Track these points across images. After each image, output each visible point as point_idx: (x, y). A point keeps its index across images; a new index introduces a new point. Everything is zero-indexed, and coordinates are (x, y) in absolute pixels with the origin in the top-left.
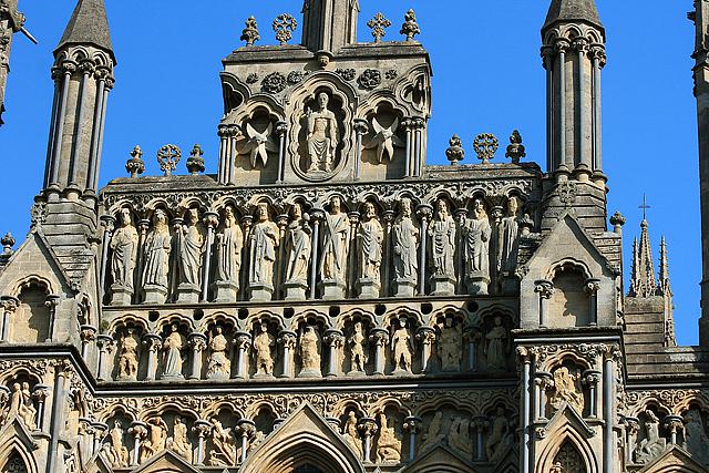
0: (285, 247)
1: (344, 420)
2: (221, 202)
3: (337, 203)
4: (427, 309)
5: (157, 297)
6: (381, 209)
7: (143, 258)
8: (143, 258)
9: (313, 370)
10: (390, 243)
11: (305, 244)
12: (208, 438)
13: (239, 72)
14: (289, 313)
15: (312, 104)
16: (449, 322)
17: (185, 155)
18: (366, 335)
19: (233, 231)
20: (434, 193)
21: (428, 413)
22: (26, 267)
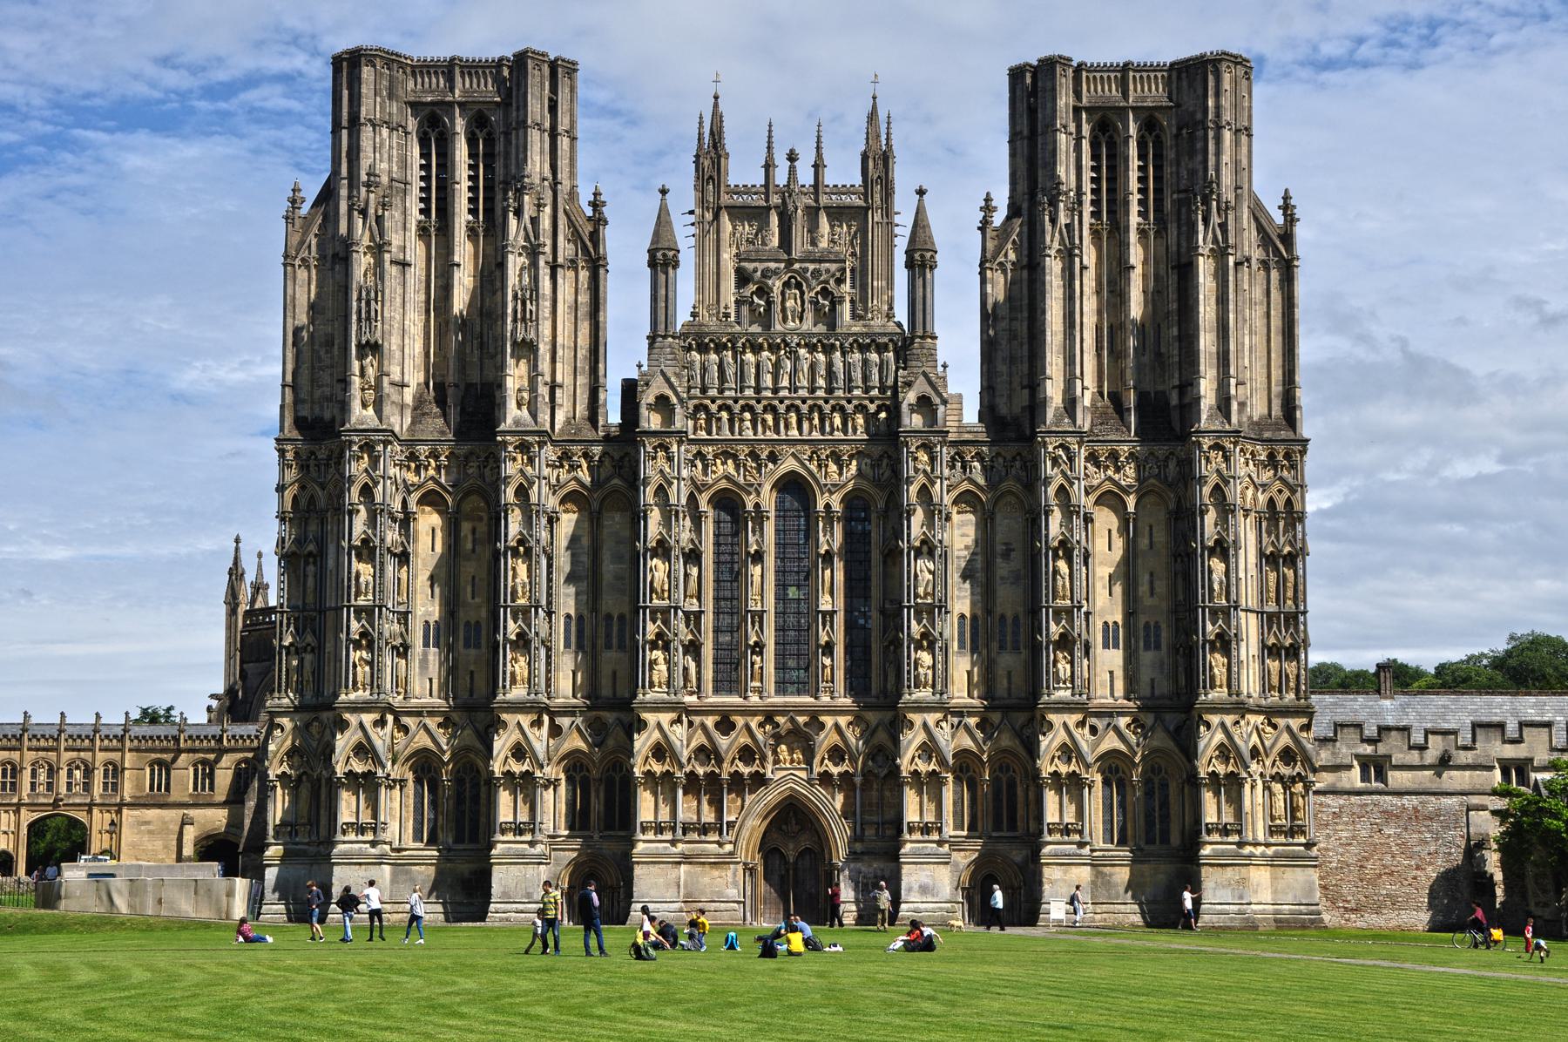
0: (777, 366)
1: (811, 459)
5: (713, 392)
6: (823, 346)
7: (704, 369)
8: (704, 369)
9: (794, 433)
10: (830, 365)
11: (788, 364)
12: (745, 465)
13: (749, 266)
15: (787, 285)
19: (749, 357)
20: (851, 340)
21: (851, 457)
22: (658, 387)
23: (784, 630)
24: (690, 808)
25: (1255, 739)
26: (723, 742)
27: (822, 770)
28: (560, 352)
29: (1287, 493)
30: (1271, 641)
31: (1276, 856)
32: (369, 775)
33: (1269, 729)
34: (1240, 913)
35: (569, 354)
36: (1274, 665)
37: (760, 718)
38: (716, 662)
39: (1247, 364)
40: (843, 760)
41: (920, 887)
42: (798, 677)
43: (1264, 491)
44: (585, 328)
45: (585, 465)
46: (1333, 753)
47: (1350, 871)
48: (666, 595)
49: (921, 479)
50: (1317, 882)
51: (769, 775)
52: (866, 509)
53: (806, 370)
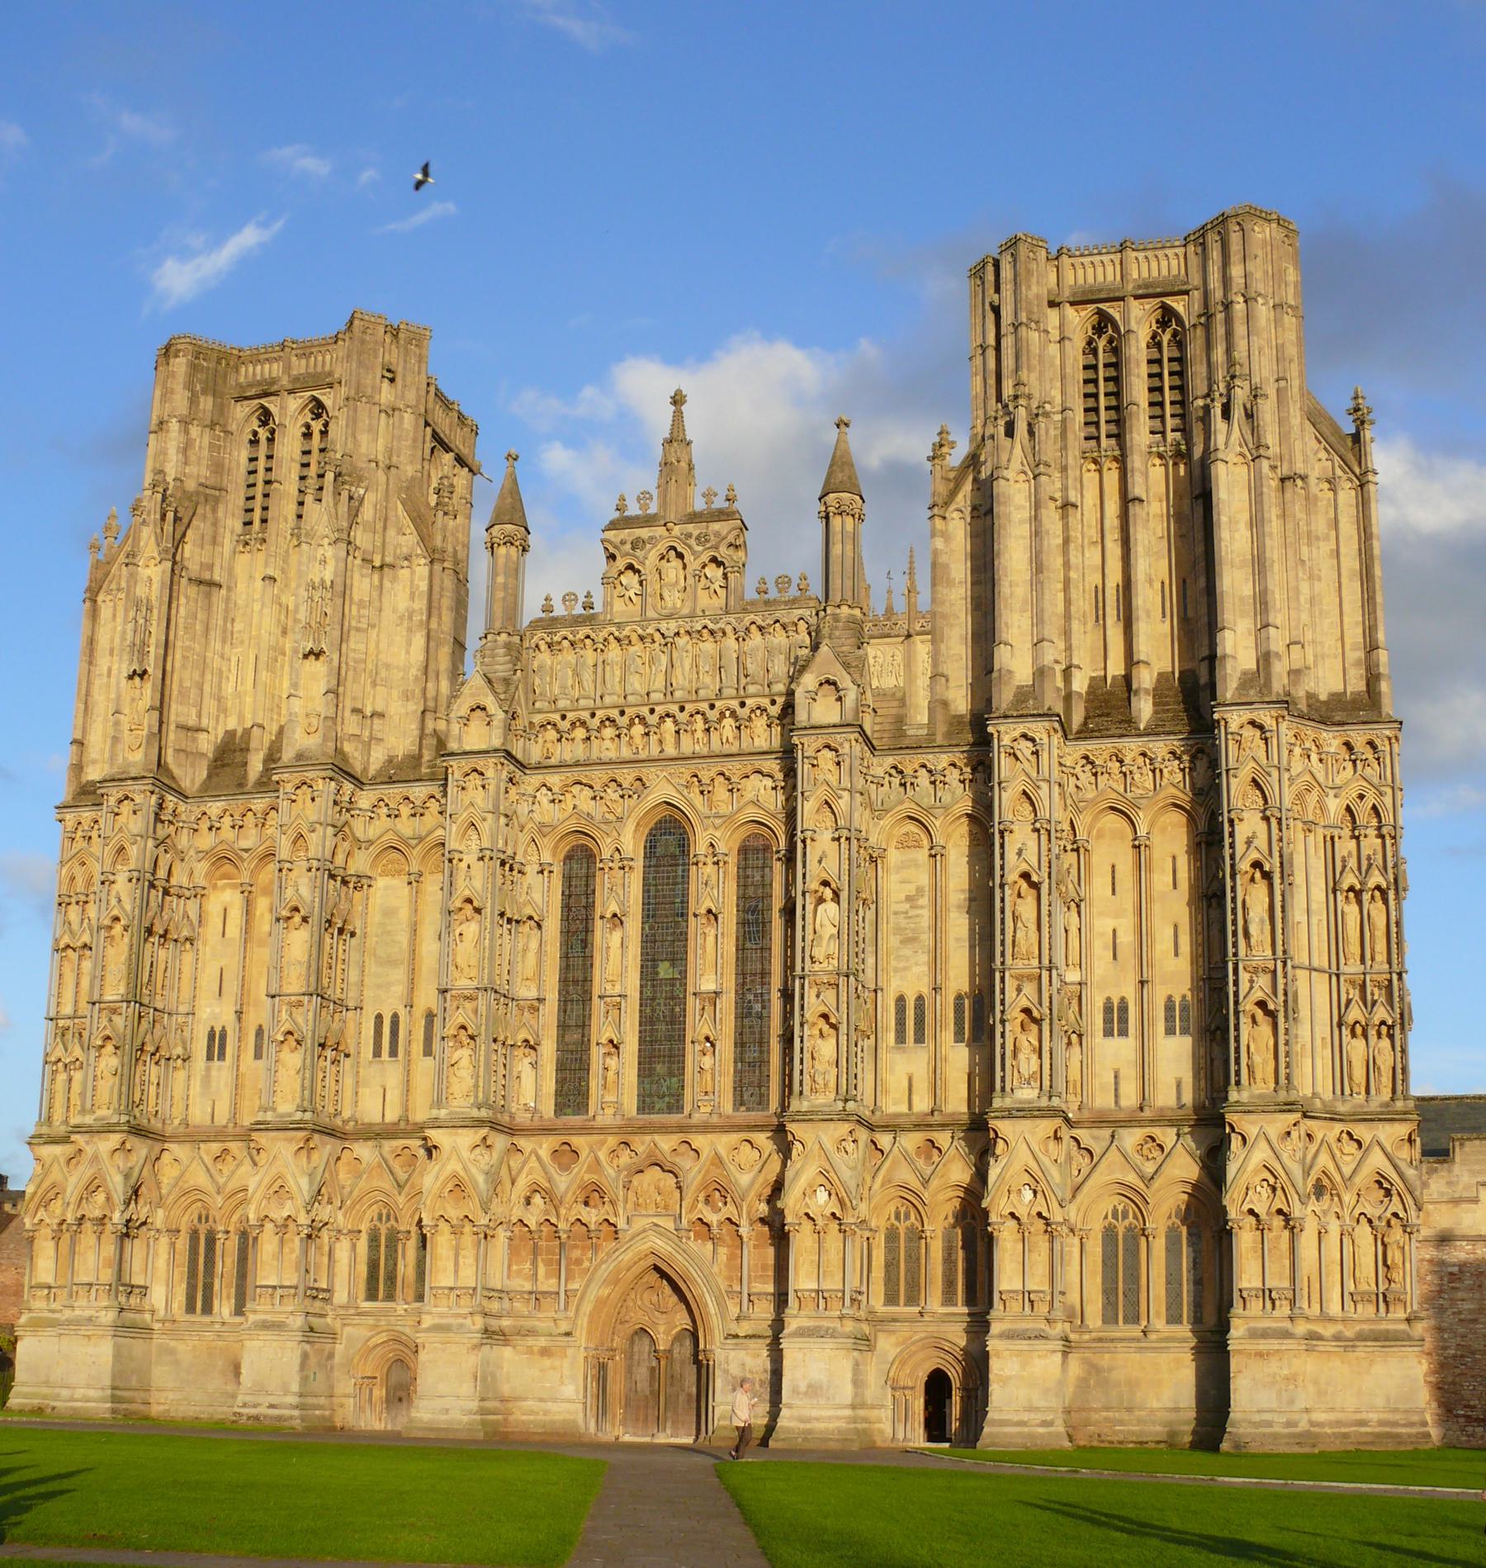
2: (604, 633)
3: (682, 631)
4: (743, 705)
6: (712, 633)
14: (652, 711)
16: (758, 712)
17: (581, 599)
18: (706, 723)
19: (614, 652)
22: (472, 695)
23: (652, 1023)
24: (519, 1272)
25: (1324, 1160)
26: (563, 1182)
27: (694, 1216)
28: (383, 674)
29: (1370, 799)
30: (1355, 1014)
31: (1361, 1337)
32: (102, 1221)
33: (1351, 1147)
34: (1289, 1424)
35: (397, 675)
36: (1357, 1049)
37: (612, 1141)
38: (561, 1067)
39: (1305, 617)
40: (726, 1203)
41: (809, 1386)
42: (668, 1088)
43: (1335, 796)
44: (419, 640)
45: (405, 810)
46: (1449, 1184)
47: (1475, 1361)
48: (473, 973)
49: (821, 793)
50: (1421, 1377)
51: (621, 1224)
52: (767, 848)
53: (687, 667)
